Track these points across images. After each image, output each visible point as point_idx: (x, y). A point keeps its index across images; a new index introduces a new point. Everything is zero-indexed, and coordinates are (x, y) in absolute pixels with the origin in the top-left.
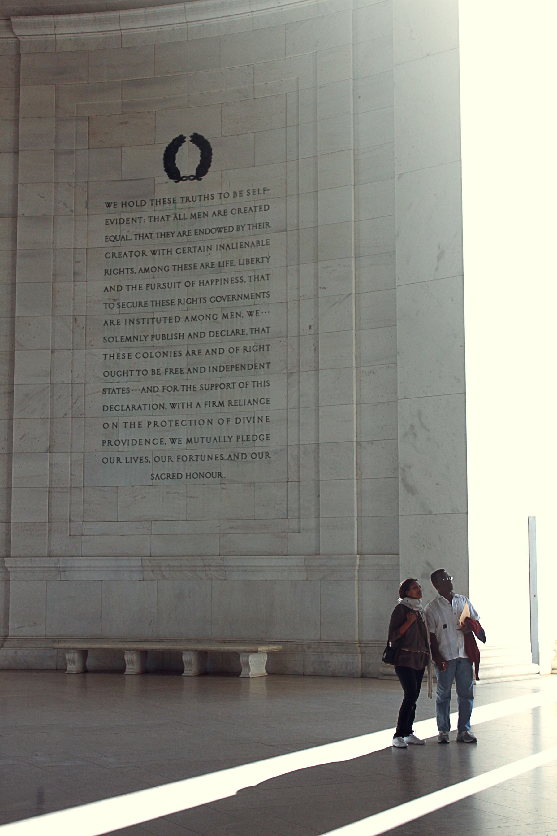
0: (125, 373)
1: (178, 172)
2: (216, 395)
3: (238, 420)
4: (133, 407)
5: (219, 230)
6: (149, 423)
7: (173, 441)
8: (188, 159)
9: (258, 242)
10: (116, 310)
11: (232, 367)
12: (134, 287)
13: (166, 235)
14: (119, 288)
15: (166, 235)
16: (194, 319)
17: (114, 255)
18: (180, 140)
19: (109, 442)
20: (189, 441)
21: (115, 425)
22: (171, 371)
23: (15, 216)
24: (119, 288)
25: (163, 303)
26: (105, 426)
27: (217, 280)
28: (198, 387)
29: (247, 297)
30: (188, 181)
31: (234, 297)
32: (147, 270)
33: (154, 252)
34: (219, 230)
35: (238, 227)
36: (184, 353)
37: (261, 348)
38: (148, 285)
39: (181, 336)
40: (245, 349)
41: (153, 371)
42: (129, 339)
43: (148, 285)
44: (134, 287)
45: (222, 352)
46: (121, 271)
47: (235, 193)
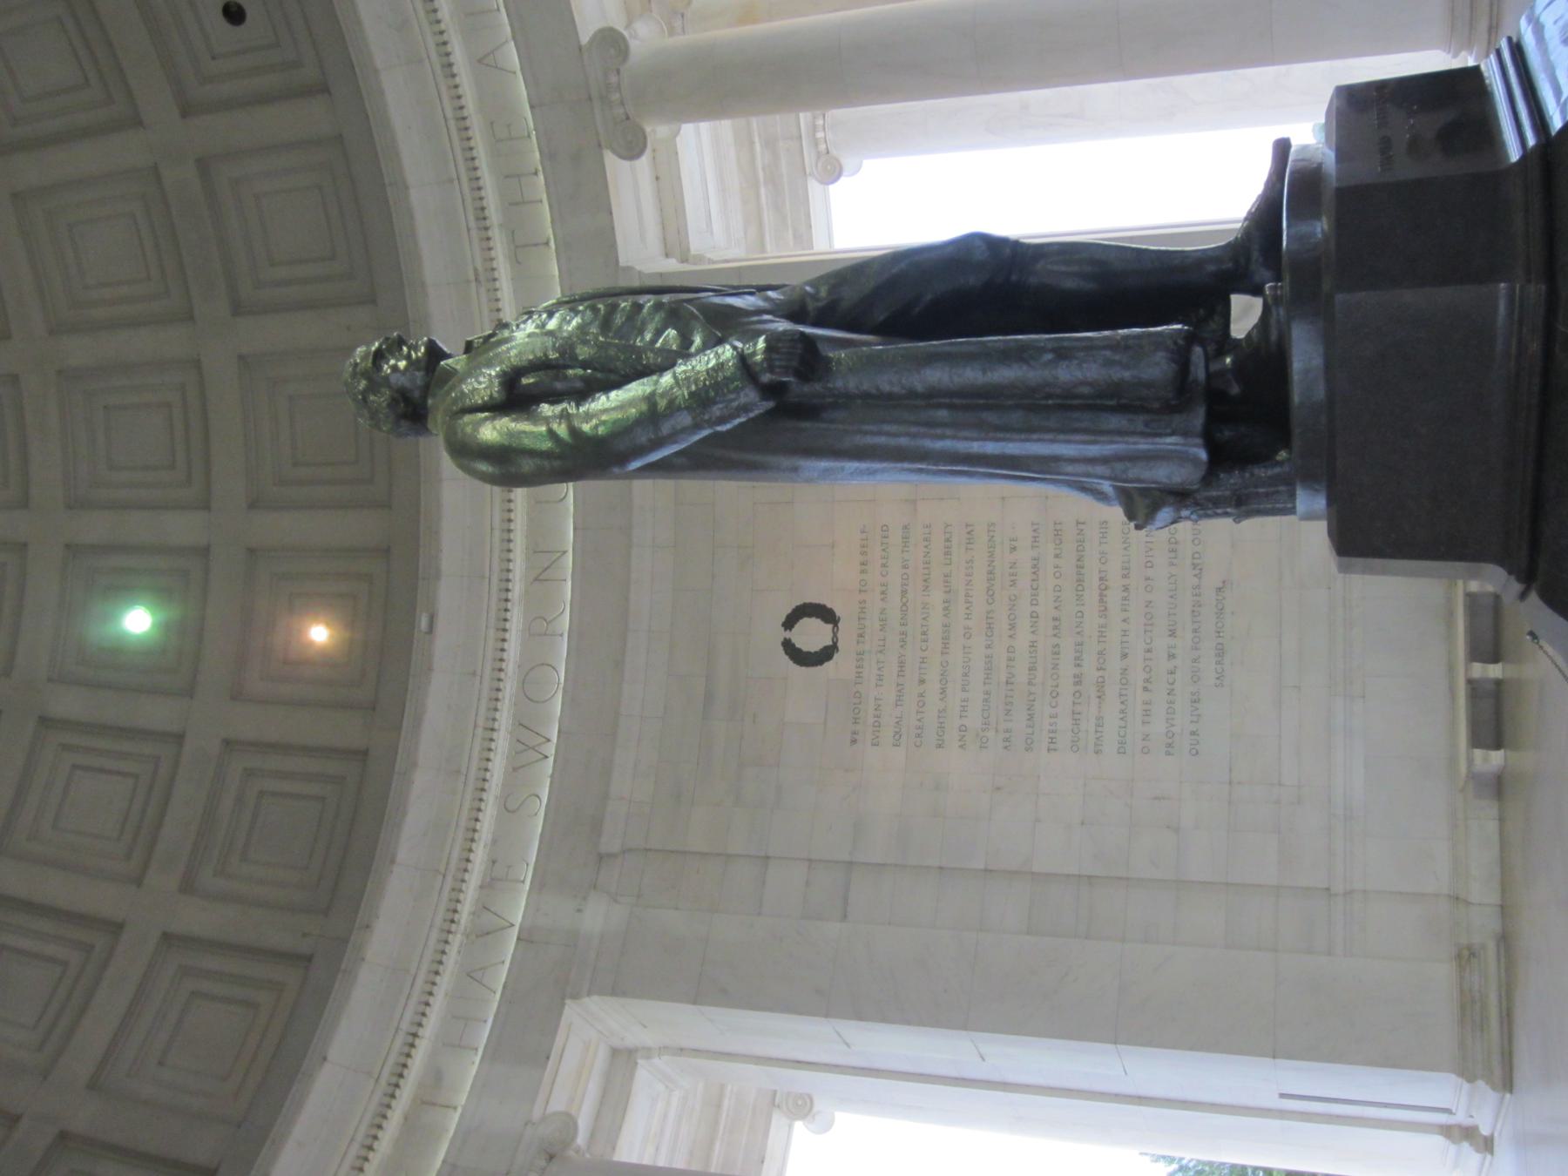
0: (1076, 722)
1: (826, 648)
2: (1114, 598)
3: (1149, 565)
4: (1122, 712)
5: (904, 593)
6: (1146, 689)
7: (1171, 656)
8: (811, 635)
9: (926, 540)
10: (991, 734)
11: (1079, 574)
12: (964, 709)
13: (902, 665)
14: (963, 729)
15: (902, 665)
16: (1012, 627)
17: (918, 736)
18: (788, 646)
19: (1169, 745)
20: (1173, 634)
21: (1146, 737)
22: (1077, 658)
23: (850, 864)
24: (963, 729)
25: (989, 669)
26: (1145, 751)
27: (967, 595)
28: (1102, 621)
29: (991, 555)
30: (839, 635)
31: (990, 573)
32: (943, 691)
33: (922, 682)
34: (904, 593)
35: (905, 567)
36: (1056, 640)
37: (1058, 534)
38: (964, 690)
39: (1033, 645)
40: (1057, 556)
41: (1076, 683)
42: (1031, 717)
43: (964, 690)
44: (964, 709)
45: (1057, 589)
46: (941, 727)
47: (862, 572)
